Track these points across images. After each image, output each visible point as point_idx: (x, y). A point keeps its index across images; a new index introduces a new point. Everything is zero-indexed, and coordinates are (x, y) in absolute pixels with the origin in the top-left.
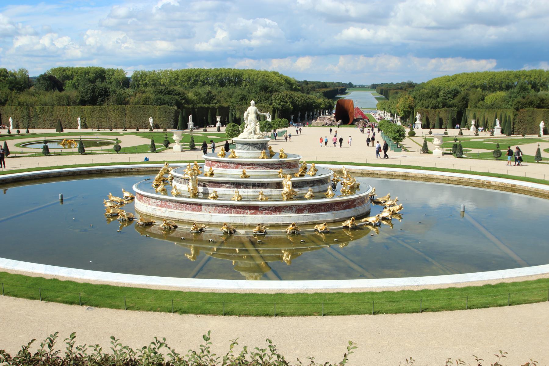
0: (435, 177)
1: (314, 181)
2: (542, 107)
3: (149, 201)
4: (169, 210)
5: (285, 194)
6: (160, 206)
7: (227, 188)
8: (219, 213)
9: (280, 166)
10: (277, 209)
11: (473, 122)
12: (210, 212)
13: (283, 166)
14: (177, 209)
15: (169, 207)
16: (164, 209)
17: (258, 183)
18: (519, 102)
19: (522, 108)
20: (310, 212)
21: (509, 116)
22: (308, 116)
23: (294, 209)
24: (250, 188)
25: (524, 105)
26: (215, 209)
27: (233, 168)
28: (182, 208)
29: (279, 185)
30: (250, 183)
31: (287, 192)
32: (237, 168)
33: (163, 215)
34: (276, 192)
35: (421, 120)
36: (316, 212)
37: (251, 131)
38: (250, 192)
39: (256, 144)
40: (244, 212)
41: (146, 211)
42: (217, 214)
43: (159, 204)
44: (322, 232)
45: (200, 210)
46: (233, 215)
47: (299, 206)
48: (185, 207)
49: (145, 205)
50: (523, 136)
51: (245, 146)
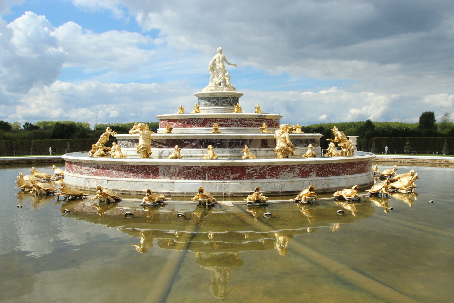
0: (386, 160)
1: (307, 140)
4: (109, 178)
5: (281, 150)
6: (96, 174)
9: (259, 123)
12: (171, 178)
14: (120, 176)
16: (101, 178)
17: (237, 140)
20: (318, 175)
23: (297, 171)
25: (373, 135)
26: (180, 173)
27: (198, 126)
30: (226, 140)
31: (283, 148)
36: (325, 176)
39: (225, 98)
40: (224, 175)
41: (76, 184)
42: (183, 181)
44: (351, 201)
47: (303, 166)
49: (75, 175)
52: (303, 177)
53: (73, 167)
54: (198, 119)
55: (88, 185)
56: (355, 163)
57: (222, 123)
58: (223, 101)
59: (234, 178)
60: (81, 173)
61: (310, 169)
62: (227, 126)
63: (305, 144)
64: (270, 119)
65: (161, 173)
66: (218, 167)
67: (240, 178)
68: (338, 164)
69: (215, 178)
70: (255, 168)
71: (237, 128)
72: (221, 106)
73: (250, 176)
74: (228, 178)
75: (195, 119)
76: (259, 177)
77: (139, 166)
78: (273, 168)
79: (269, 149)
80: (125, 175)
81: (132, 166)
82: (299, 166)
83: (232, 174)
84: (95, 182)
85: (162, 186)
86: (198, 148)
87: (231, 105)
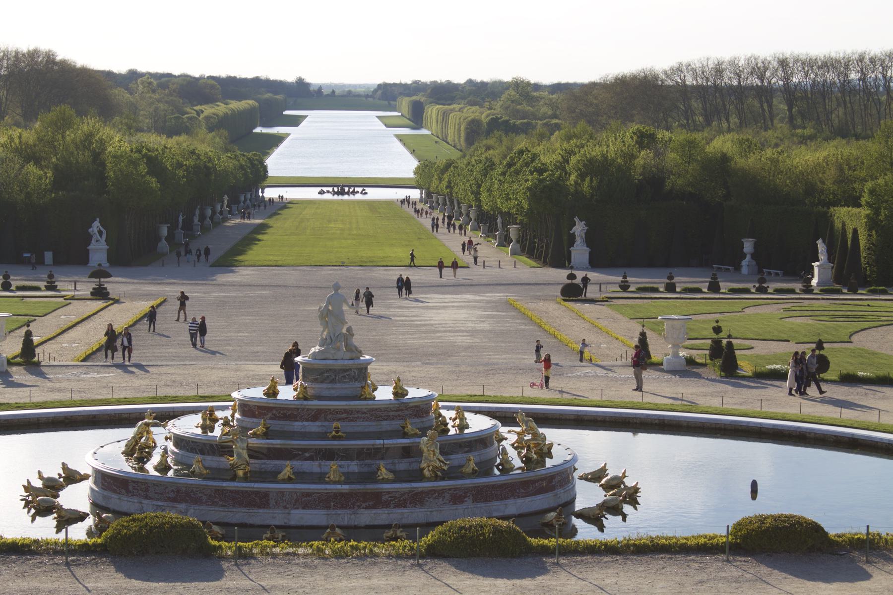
1: (470, 442)
6: (175, 500)
8: (304, 508)
9: (400, 413)
10: (417, 499)
11: (748, 246)
12: (285, 507)
13: (407, 412)
16: (182, 506)
17: (368, 449)
20: (475, 500)
21: (855, 231)
22: (202, 218)
24: (352, 459)
26: (297, 501)
27: (307, 420)
29: (409, 452)
34: (403, 465)
35: (589, 240)
36: (486, 501)
38: (354, 466)
39: (348, 370)
42: (301, 511)
43: (172, 495)
47: (456, 489)
52: (455, 503)
53: (130, 488)
54: (308, 410)
56: (530, 481)
57: (344, 415)
58: (341, 375)
59: (366, 508)
60: (147, 497)
61: (465, 493)
62: (352, 421)
63: (466, 449)
64: (416, 406)
65: (272, 502)
66: (347, 494)
67: (374, 507)
68: (505, 484)
69: (342, 507)
70: (393, 494)
71: (367, 423)
72: (340, 382)
73: (386, 505)
74: (359, 507)
75: (303, 409)
76: (398, 506)
77: (242, 491)
78: (416, 494)
79: (412, 459)
80: (221, 503)
81: (232, 492)
82: (450, 489)
83: (364, 502)
85: (274, 518)
86: (313, 460)
87: (356, 380)
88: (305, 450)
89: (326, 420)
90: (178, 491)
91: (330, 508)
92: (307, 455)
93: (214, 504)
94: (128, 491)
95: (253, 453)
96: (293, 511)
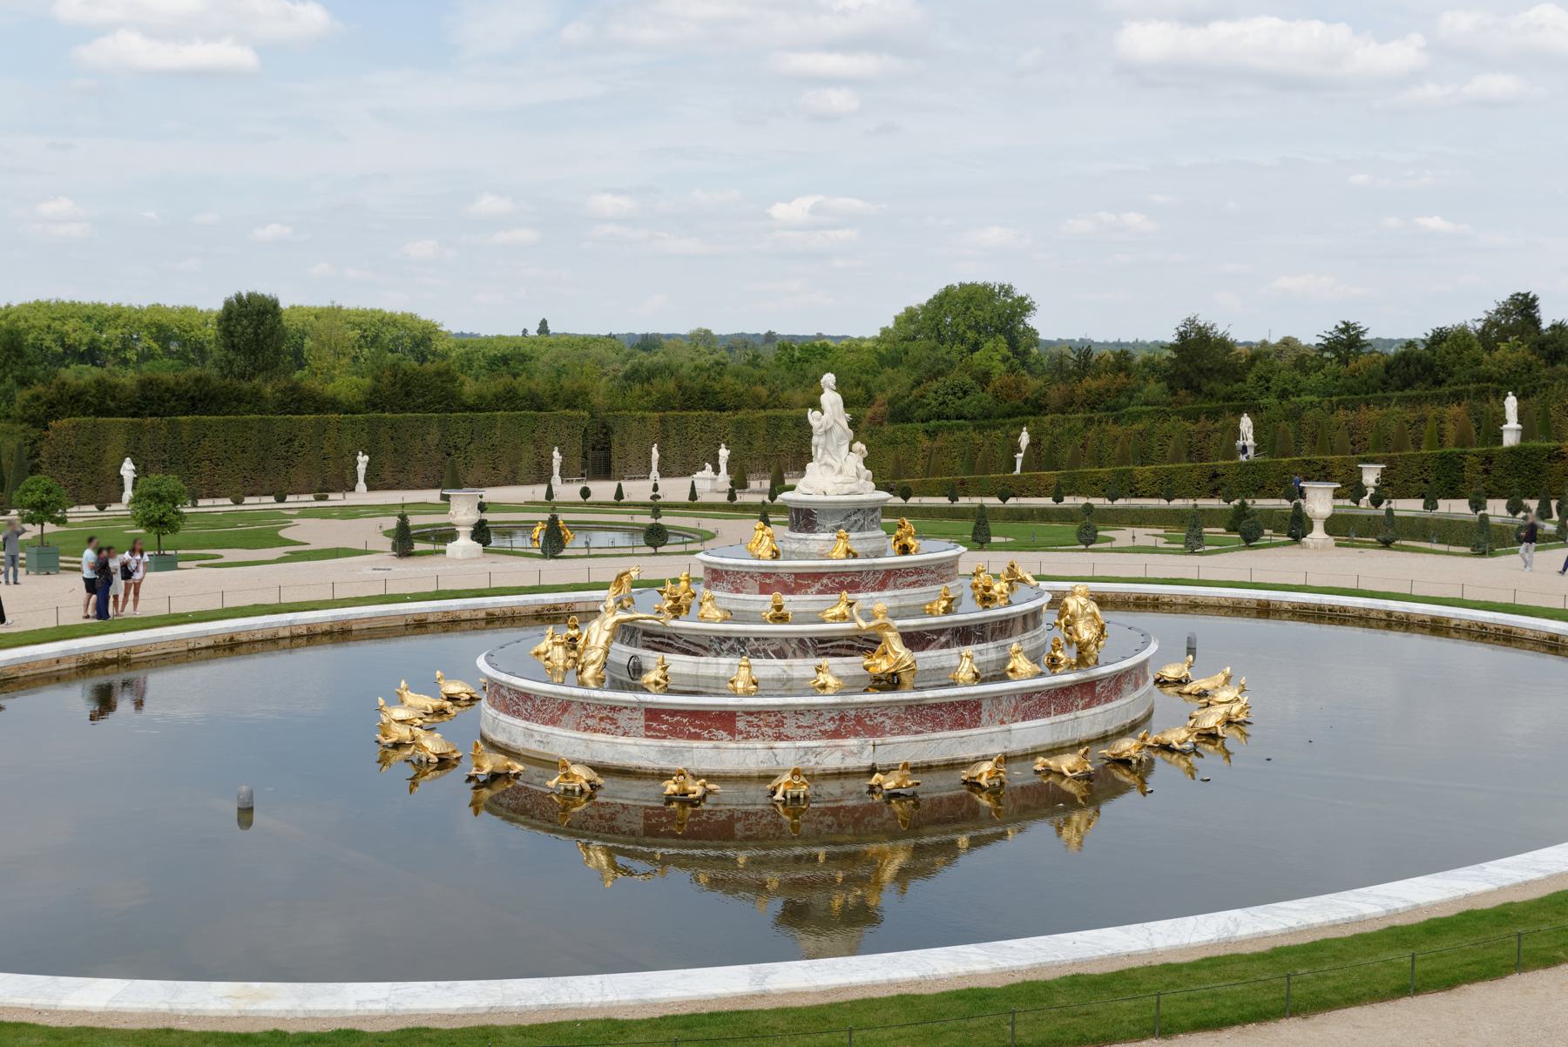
2: (109, 413)
3: (780, 724)
4: (878, 741)
6: (835, 734)
7: (942, 647)
12: (1002, 722)
15: (874, 731)
16: (852, 742)
18: (37, 398)
19: (50, 417)
26: (1016, 709)
27: (873, 590)
28: (921, 724)
32: (882, 586)
33: (851, 763)
37: (836, 471)
41: (764, 767)
43: (830, 726)
45: (975, 723)
46: (1053, 719)
48: (933, 720)
49: (759, 745)
50: (101, 509)
51: (853, 518)
55: (811, 764)
57: (914, 578)
60: (779, 737)
65: (985, 716)
81: (931, 707)
84: (838, 754)
88: (940, 632)
89: (896, 587)
90: (842, 719)
91: (1049, 714)
92: (943, 639)
93: (903, 731)
94: (732, 732)
95: (914, 640)
96: (1014, 726)
